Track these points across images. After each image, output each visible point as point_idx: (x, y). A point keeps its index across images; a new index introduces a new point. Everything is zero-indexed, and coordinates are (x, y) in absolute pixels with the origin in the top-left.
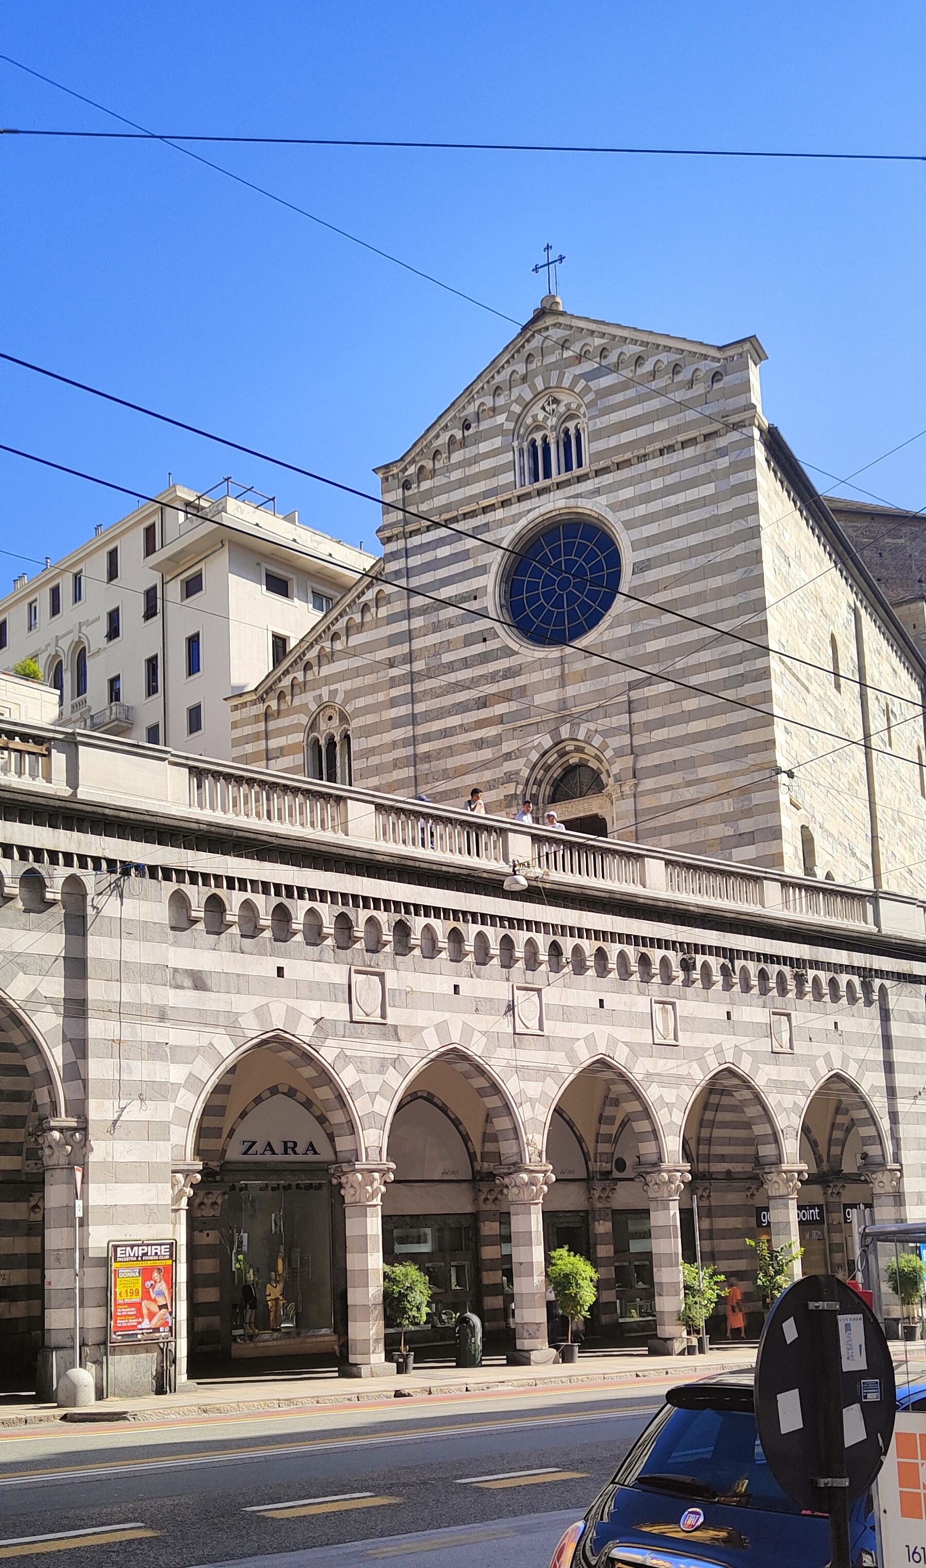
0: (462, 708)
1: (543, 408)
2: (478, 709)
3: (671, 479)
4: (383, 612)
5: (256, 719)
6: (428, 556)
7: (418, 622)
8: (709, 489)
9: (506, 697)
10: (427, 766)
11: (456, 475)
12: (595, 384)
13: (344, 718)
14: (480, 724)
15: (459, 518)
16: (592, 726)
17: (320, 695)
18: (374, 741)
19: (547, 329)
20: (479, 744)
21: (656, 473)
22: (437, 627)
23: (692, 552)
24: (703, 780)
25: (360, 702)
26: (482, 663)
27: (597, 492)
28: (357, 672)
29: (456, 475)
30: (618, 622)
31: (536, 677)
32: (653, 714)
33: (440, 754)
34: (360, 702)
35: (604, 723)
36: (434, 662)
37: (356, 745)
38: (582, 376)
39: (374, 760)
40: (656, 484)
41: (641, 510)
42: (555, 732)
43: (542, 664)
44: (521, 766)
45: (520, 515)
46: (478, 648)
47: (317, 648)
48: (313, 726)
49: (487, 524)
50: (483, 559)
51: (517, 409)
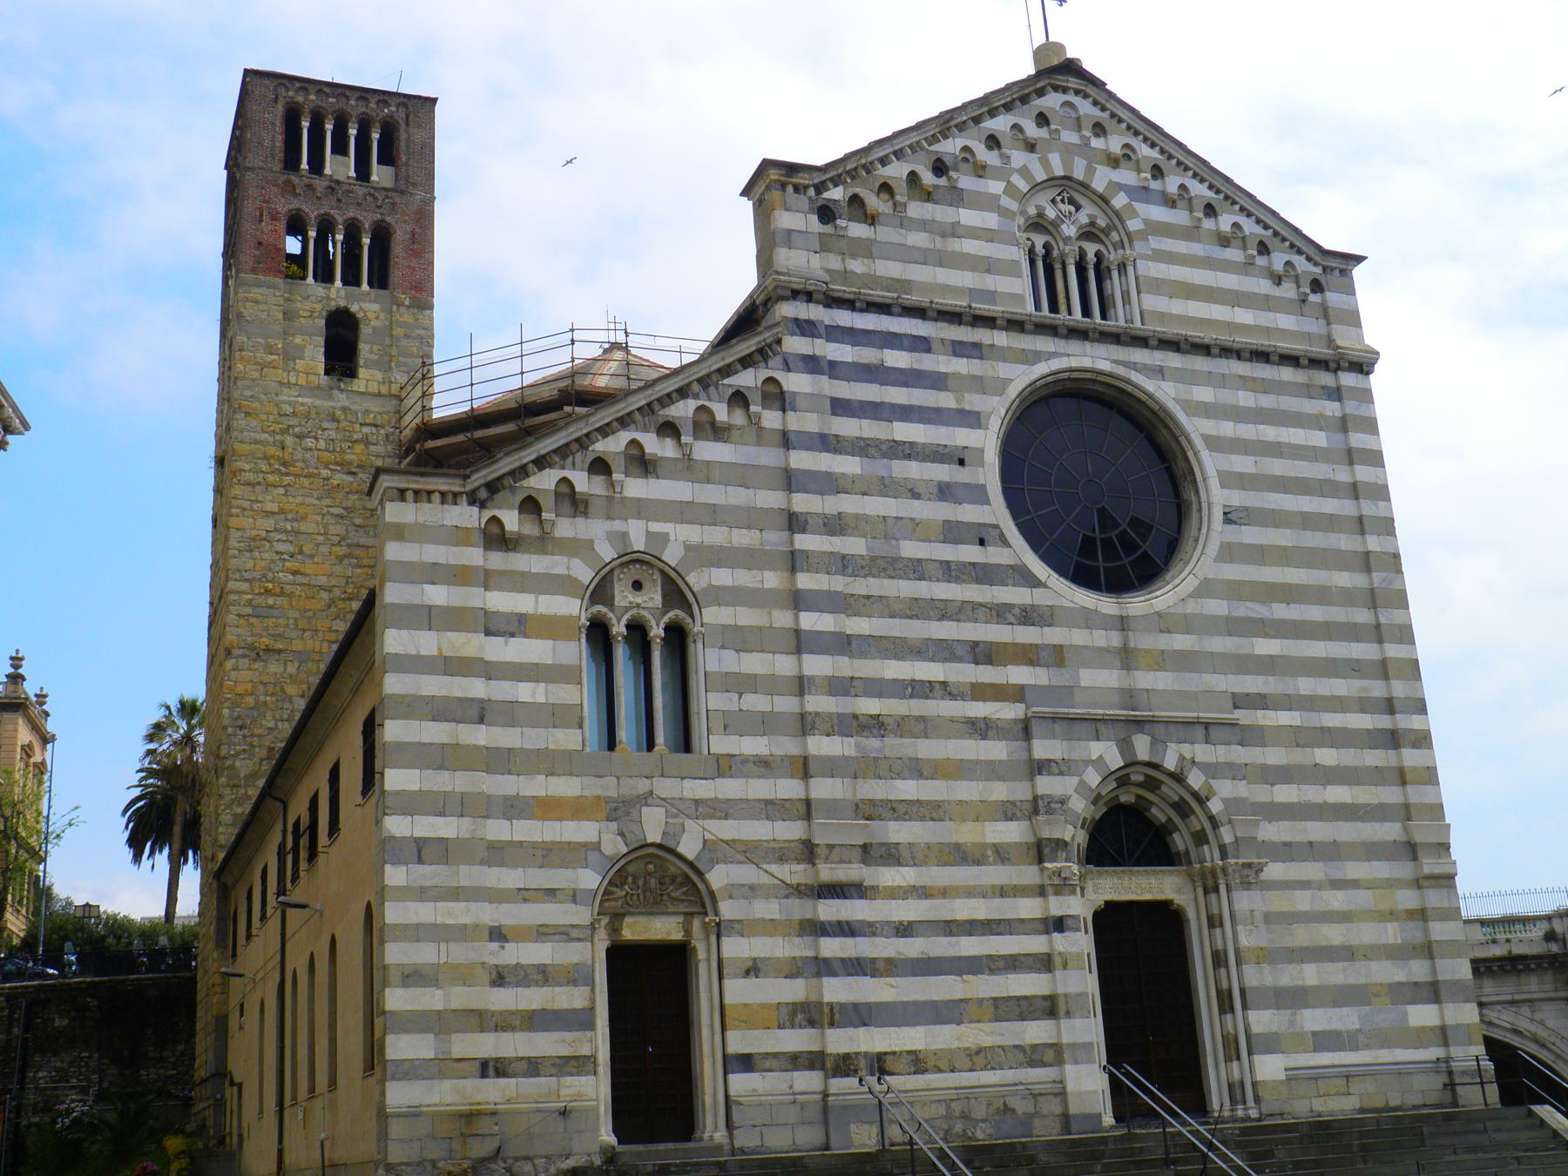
0: (944, 651)
1: (1053, 201)
2: (976, 662)
3: (1267, 401)
4: (771, 419)
5: (460, 536)
6: (867, 355)
7: (848, 465)
8: (1319, 439)
9: (1028, 655)
10: (872, 743)
11: (917, 239)
12: (1138, 206)
13: (675, 593)
14: (980, 692)
15: (930, 314)
16: (1186, 749)
17: (624, 536)
18: (754, 663)
19: (1065, 90)
20: (981, 729)
21: (1245, 383)
22: (886, 487)
23: (1308, 521)
24: (1354, 884)
25: (722, 577)
26: (979, 581)
27: (1160, 372)
28: (712, 515)
29: (917, 239)
30: (1206, 589)
31: (1077, 637)
32: (1274, 756)
33: (903, 727)
34: (722, 577)
35: (1202, 752)
36: (882, 549)
37: (708, 660)
38: (1120, 187)
39: (755, 702)
40: (1245, 399)
41: (1228, 429)
42: (1125, 746)
43: (1088, 619)
44: (1070, 791)
45: (1036, 357)
46: (970, 553)
47: (624, 437)
48: (601, 592)
49: (976, 346)
50: (973, 402)
51: (1023, 186)
